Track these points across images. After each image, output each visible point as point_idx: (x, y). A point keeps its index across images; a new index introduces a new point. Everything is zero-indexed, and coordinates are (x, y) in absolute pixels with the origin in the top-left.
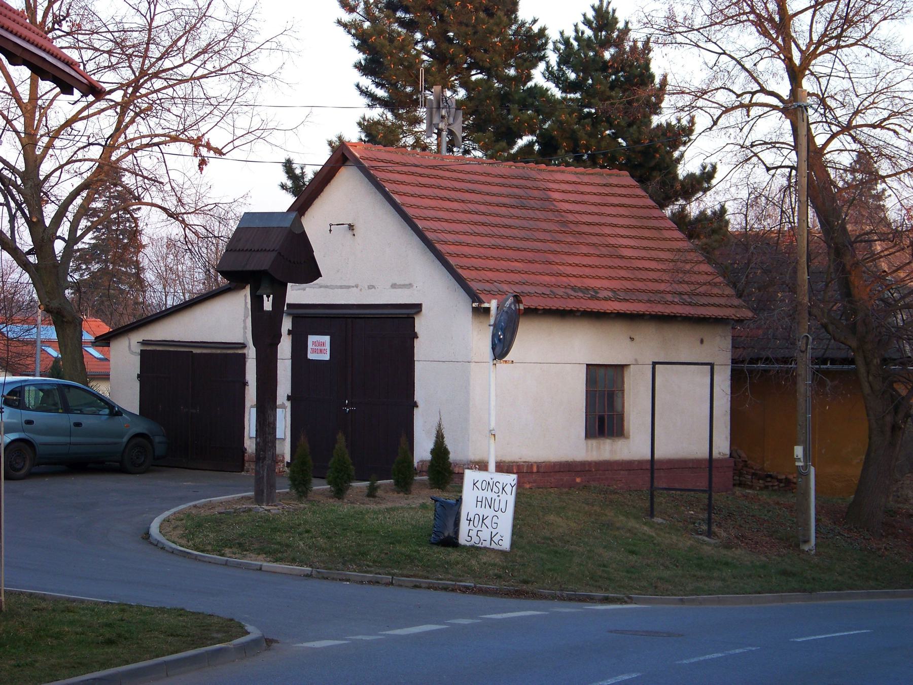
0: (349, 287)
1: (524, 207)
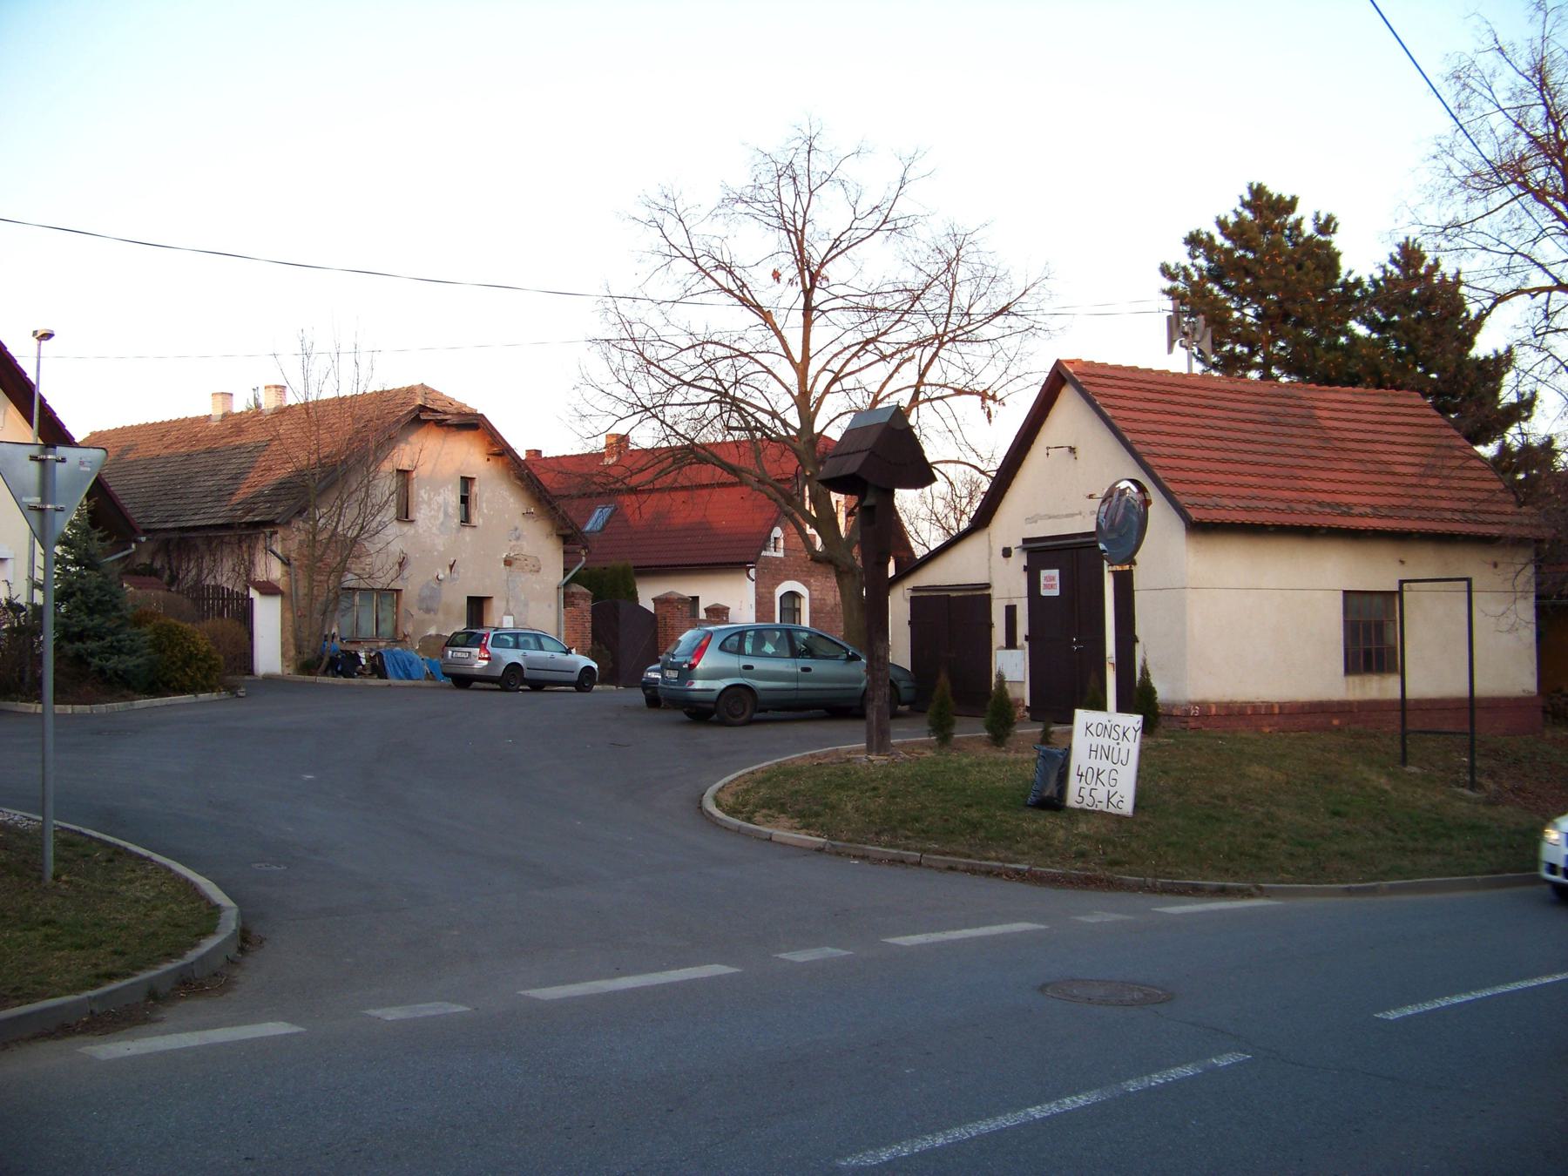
0: (1072, 515)
1: (1278, 424)
